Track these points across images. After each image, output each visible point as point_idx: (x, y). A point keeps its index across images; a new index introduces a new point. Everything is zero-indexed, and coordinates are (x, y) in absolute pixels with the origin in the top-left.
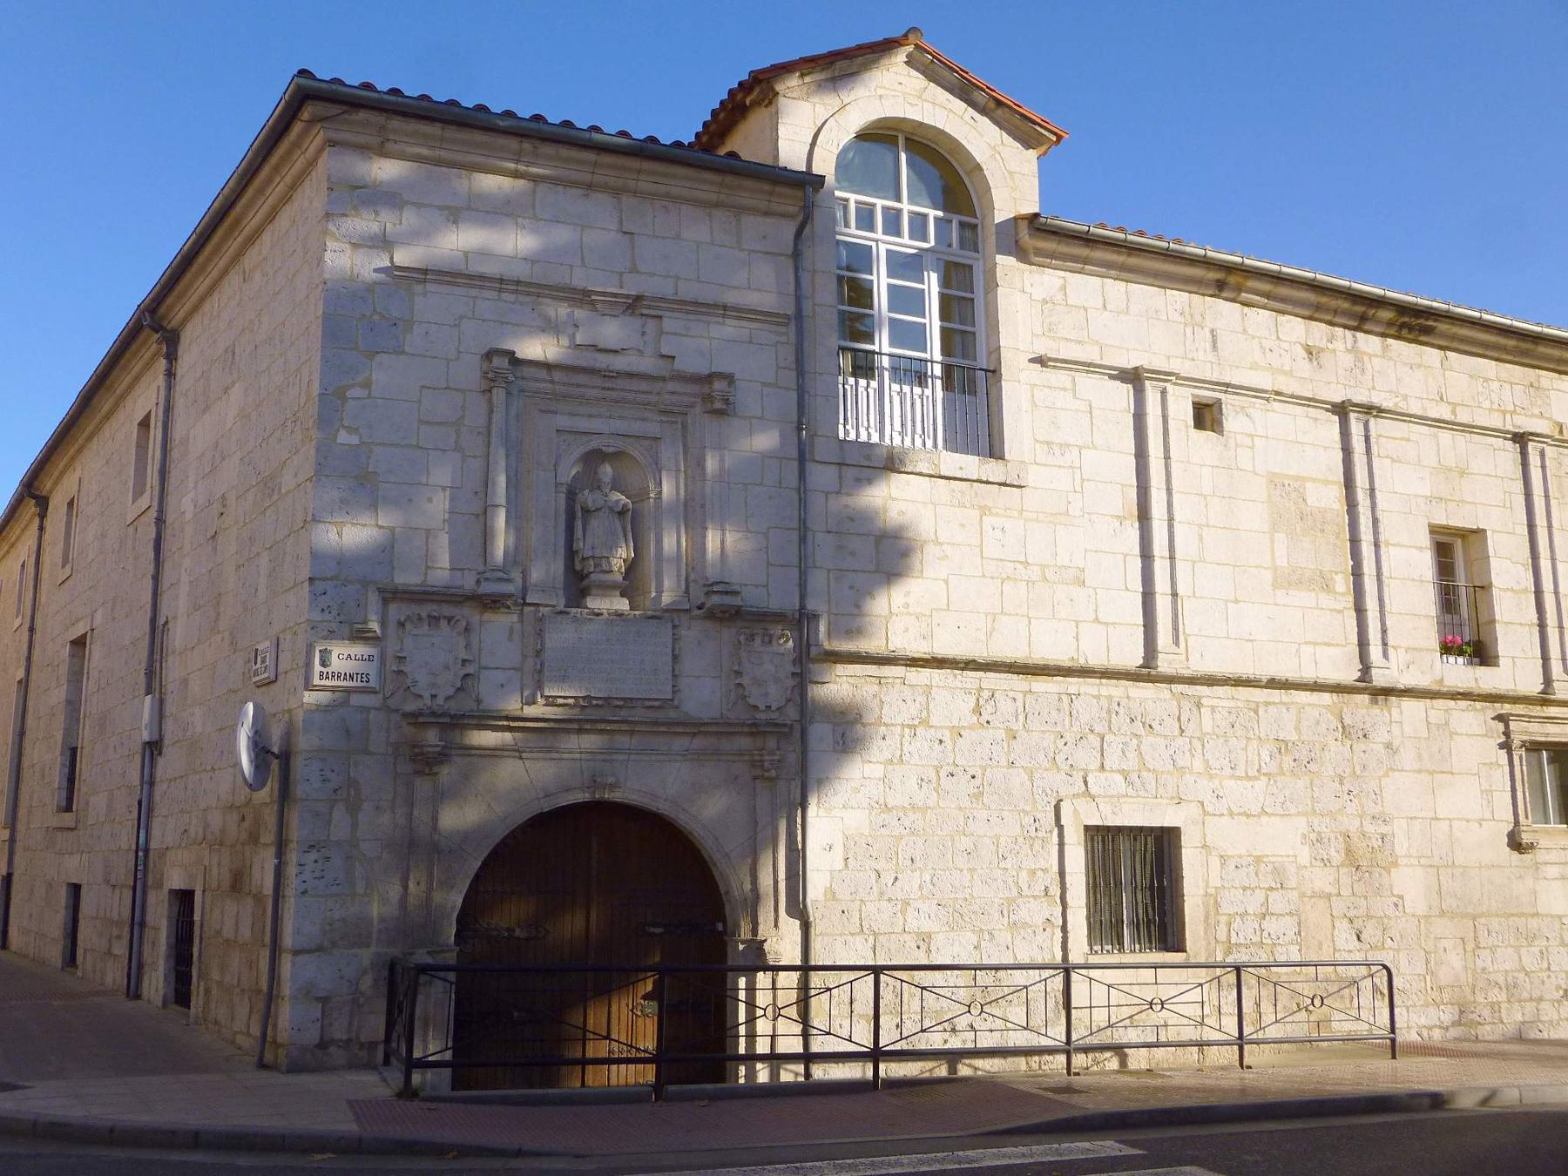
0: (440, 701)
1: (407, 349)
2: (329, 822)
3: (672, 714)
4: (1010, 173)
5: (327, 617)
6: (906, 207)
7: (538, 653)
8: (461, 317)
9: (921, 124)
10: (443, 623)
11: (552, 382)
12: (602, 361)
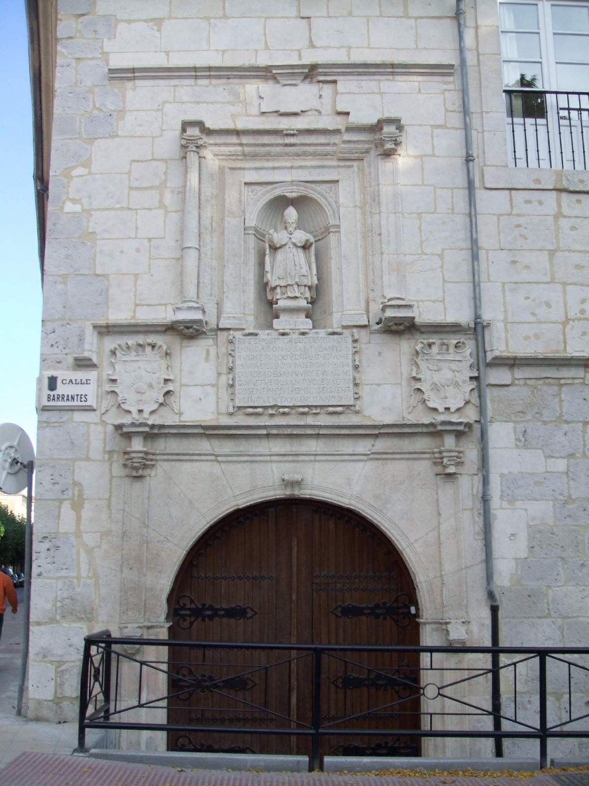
0: (146, 414)
1: (120, 133)
3: (355, 420)
5: (55, 350)
7: (231, 369)
8: (164, 102)
10: (148, 349)
11: (241, 145)
12: (284, 124)
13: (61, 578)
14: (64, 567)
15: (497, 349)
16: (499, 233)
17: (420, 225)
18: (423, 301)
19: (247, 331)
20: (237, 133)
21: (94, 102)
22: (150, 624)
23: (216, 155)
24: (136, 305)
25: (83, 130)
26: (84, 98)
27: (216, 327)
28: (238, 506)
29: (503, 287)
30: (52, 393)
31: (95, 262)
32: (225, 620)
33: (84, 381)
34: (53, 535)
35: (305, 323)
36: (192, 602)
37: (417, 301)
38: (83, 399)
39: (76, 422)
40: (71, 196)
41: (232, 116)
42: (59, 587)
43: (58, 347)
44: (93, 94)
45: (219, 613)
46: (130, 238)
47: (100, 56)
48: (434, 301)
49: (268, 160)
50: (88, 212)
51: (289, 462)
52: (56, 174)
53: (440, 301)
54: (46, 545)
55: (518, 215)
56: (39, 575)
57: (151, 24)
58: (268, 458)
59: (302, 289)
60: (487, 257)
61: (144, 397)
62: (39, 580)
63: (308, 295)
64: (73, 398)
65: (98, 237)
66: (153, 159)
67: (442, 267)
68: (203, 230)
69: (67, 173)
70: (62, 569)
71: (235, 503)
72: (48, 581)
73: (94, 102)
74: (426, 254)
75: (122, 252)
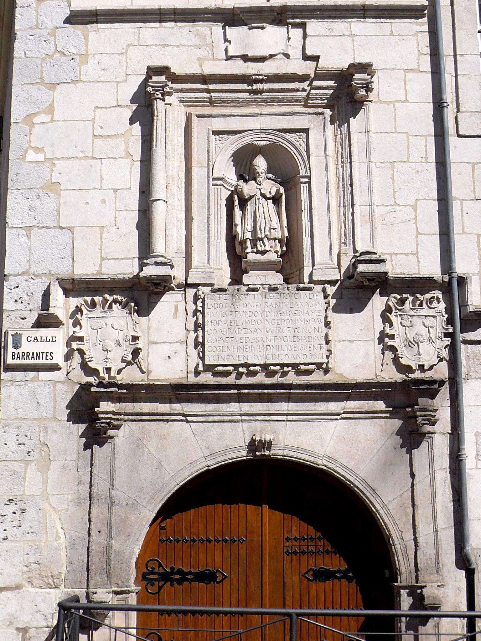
2: (24, 478)
3: (329, 378)
5: (19, 306)
8: (129, 45)
12: (252, 69)
15: (471, 305)
16: (474, 182)
17: (393, 174)
18: (396, 255)
19: (216, 287)
20: (204, 79)
22: (119, 590)
23: (181, 102)
24: (103, 259)
26: (45, 41)
27: (184, 282)
28: (208, 466)
30: (16, 351)
31: (58, 214)
35: (277, 279)
36: (160, 565)
37: (391, 255)
38: (49, 357)
40: (33, 145)
41: (199, 59)
43: (22, 302)
48: (407, 255)
49: (235, 106)
50: (51, 161)
51: (261, 421)
52: (18, 121)
58: (239, 418)
59: (272, 243)
60: (462, 207)
61: (110, 355)
62: (4, 544)
63: (278, 248)
67: (415, 218)
68: (170, 181)
69: (29, 119)
70: (28, 533)
71: (206, 464)
72: (14, 544)
74: (399, 205)
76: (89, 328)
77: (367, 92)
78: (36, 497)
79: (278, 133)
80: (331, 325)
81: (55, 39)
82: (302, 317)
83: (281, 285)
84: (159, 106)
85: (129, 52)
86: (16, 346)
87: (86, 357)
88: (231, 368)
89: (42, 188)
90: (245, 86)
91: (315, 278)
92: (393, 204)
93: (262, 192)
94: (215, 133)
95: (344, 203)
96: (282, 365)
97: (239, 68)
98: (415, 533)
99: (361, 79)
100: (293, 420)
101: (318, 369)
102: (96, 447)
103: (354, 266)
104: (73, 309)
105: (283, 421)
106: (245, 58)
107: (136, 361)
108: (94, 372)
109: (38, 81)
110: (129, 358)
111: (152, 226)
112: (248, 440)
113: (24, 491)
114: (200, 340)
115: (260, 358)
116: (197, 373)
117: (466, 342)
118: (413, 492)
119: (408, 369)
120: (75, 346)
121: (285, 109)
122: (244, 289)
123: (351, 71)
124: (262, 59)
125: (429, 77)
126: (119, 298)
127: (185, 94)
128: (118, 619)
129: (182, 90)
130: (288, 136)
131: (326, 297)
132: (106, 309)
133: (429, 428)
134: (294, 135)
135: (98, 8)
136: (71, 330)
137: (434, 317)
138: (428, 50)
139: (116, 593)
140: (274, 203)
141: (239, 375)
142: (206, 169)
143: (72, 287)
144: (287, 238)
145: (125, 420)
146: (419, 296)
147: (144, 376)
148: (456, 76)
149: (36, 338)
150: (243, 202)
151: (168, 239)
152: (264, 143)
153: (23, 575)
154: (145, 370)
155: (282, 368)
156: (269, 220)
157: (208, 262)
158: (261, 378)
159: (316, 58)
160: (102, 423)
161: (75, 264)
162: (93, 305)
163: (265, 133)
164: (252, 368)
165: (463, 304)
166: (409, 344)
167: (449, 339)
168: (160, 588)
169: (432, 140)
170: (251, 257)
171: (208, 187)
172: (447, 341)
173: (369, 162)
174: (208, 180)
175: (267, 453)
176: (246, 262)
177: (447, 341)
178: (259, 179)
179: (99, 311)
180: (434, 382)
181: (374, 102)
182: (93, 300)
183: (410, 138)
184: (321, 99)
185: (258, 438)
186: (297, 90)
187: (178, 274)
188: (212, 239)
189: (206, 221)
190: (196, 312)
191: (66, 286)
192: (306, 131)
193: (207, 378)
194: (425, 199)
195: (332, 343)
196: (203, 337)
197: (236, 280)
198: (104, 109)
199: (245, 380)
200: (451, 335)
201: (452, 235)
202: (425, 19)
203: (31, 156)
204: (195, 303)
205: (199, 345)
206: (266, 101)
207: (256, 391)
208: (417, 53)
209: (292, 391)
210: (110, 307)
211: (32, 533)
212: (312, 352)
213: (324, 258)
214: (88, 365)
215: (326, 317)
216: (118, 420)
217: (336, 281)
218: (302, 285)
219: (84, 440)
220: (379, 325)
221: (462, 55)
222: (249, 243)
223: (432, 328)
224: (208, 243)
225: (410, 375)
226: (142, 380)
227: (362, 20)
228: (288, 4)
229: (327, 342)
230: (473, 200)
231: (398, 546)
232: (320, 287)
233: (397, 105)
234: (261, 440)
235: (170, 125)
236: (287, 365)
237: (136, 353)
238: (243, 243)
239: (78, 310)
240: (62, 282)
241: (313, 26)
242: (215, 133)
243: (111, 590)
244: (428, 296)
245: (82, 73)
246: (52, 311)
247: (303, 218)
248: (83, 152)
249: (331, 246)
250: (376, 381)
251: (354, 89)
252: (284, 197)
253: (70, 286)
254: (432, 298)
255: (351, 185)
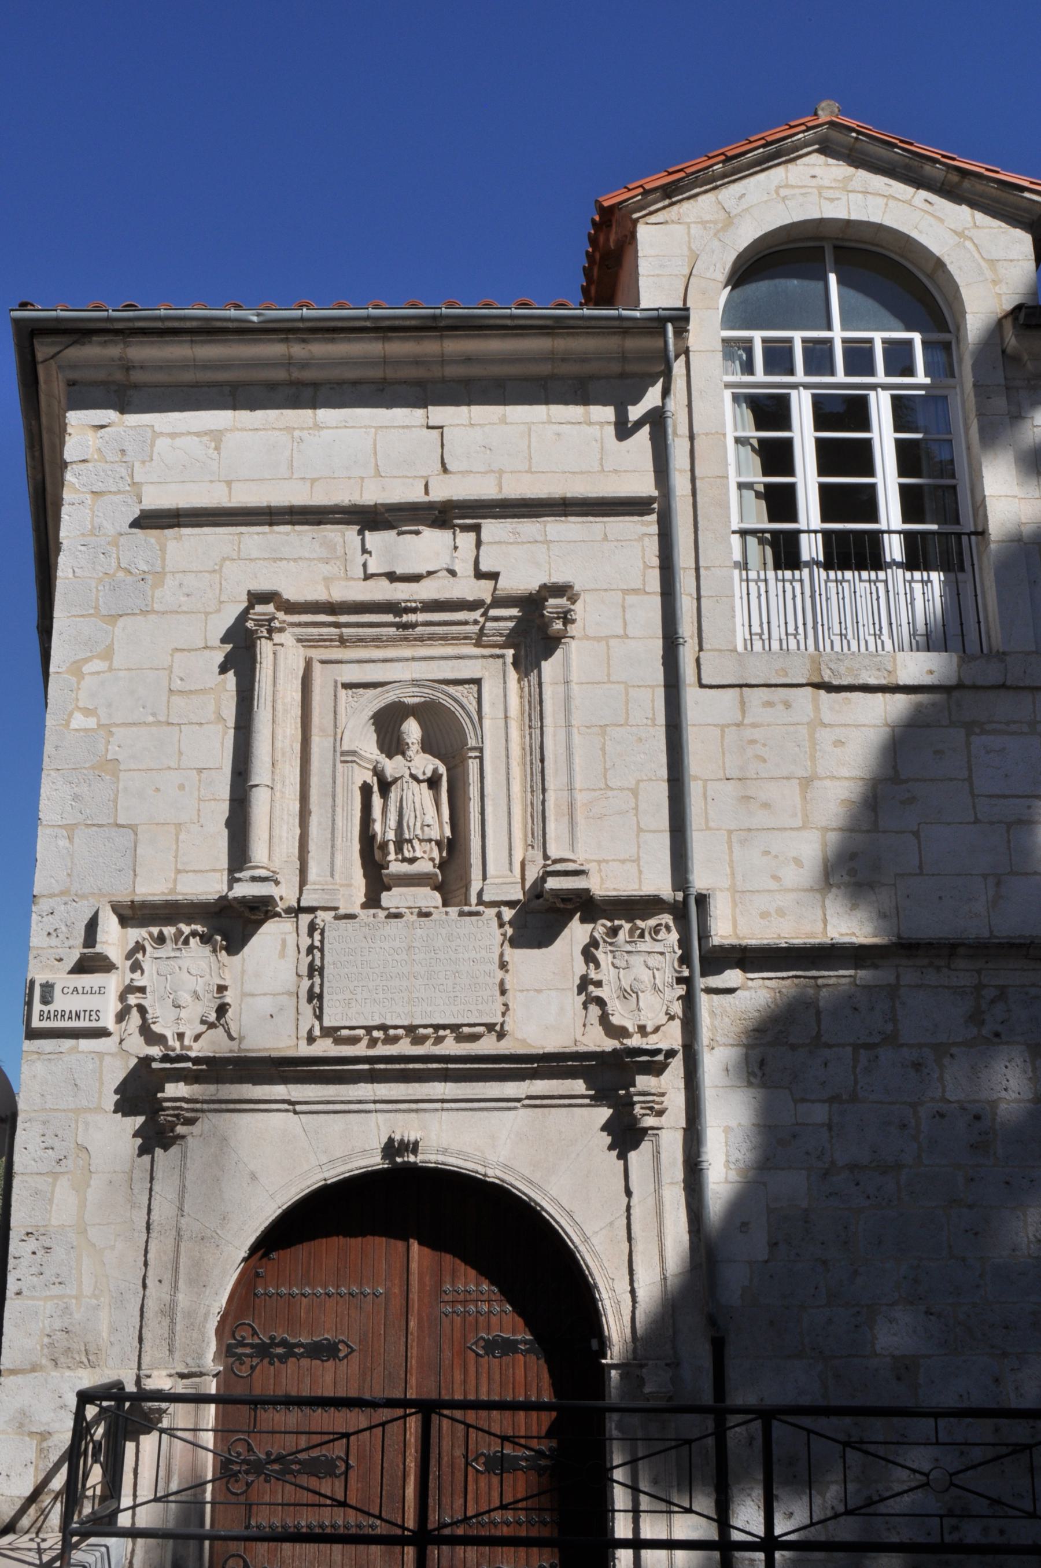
2: (51, 1200)
3: (504, 1047)
4: (992, 263)
5: (53, 941)
6: (838, 334)
8: (224, 559)
9: (848, 223)
12: (401, 592)
13: (52, 1297)
14: (57, 1281)
16: (723, 753)
17: (604, 744)
19: (342, 911)
20: (332, 608)
21: (118, 558)
23: (299, 641)
24: (178, 871)
25: (101, 602)
27: (296, 905)
29: (730, 838)
30: (46, 1008)
32: (305, 1362)
33: (96, 989)
34: (42, 1230)
37: (599, 862)
38: (94, 1017)
39: (83, 1052)
40: (81, 704)
42: (48, 1313)
44: (117, 546)
45: (296, 1350)
46: (169, 768)
47: (128, 488)
48: (623, 861)
49: (377, 647)
50: (107, 729)
52: (60, 670)
53: (633, 861)
54: (32, 1244)
55: (754, 725)
56: (19, 1294)
57: (205, 438)
58: (371, 1106)
59: (427, 846)
61: (183, 1014)
62: (17, 1301)
63: (436, 854)
64: (78, 1016)
65: (122, 767)
66: (206, 647)
67: (636, 808)
68: (279, 756)
69: (76, 669)
71: (321, 1176)
72: (30, 1302)
73: (118, 558)
74: (612, 789)
75: (157, 790)
76: (155, 974)
77: (565, 624)
78: (68, 1229)
79: (436, 685)
80: (509, 967)
81: (118, 551)
82: (466, 956)
83: (437, 908)
84: (265, 649)
85: (224, 570)
86: (46, 1000)
87: (149, 1016)
88: (362, 1032)
89: (93, 768)
90: (389, 618)
91: (486, 898)
92: (603, 786)
93: (413, 772)
94: (346, 686)
95: (532, 787)
96: (437, 1027)
97: (382, 591)
98: (632, 1282)
99: (557, 606)
100: (452, 1109)
101: (489, 1032)
102: (159, 1152)
103: (542, 879)
104: (131, 945)
105: (437, 1110)
106: (392, 577)
107: (222, 1021)
108: (159, 1039)
109: (92, 611)
110: (212, 1017)
111: (249, 824)
112: (384, 1140)
113: (49, 1220)
114: (317, 990)
115: (403, 1016)
116: (311, 1039)
117: (709, 991)
118: (628, 1218)
119: (621, 1032)
120: (132, 1000)
121: (449, 651)
122: (381, 914)
123: (544, 593)
124: (416, 578)
125: (657, 600)
126: (199, 928)
127: (304, 630)
128: (178, 1415)
129: (299, 625)
130: (451, 689)
131: (501, 925)
132: (180, 945)
133: (649, 1121)
134: (460, 688)
135: (180, 506)
136: (129, 975)
137: (662, 954)
138: (656, 562)
139: (182, 1376)
140: (430, 787)
141: (373, 1043)
142: (332, 739)
143: (132, 914)
144: (448, 838)
145: (202, 1111)
146: (639, 923)
147: (234, 1045)
148: (699, 599)
149: (76, 989)
150: (385, 786)
151: (272, 842)
152: (417, 700)
153: (42, 1348)
154: (234, 1034)
155: (436, 1032)
156: (425, 814)
157: (332, 875)
158: (405, 1047)
159: (494, 576)
160: (167, 1115)
161: (138, 879)
162: (161, 939)
163: (419, 686)
164: (392, 1032)
165: (704, 935)
166: (624, 994)
167: (684, 987)
168: (253, 1368)
169: (660, 692)
170: (396, 867)
171: (334, 766)
172: (681, 990)
173: (569, 726)
174: (334, 755)
175: (412, 1159)
176: (388, 875)
177: (681, 990)
178: (409, 753)
179: (170, 948)
180: (658, 1051)
181: (580, 639)
182: (161, 933)
183: (630, 690)
184: (501, 635)
185: (397, 1137)
186: (466, 623)
187: (286, 893)
188: (339, 842)
189: (330, 815)
190: (310, 950)
191: (122, 912)
192: (478, 682)
193: (325, 1048)
194: (651, 780)
195: (510, 994)
196: (322, 985)
197: (372, 901)
198: (186, 653)
199: (381, 1050)
200: (687, 981)
201: (688, 833)
202: (654, 517)
203: (79, 721)
204: (311, 934)
205: (315, 997)
206: (421, 639)
207: (397, 1066)
208: (641, 565)
209: (450, 1066)
210: (186, 942)
211: (60, 1283)
212: (480, 1007)
213: (502, 870)
214: (151, 1029)
215: (502, 955)
216: (193, 1110)
217: (518, 902)
218: (466, 909)
219: (139, 1141)
220: (580, 966)
221: (707, 568)
222: (392, 847)
223: (658, 969)
224: (333, 847)
225: (625, 1041)
226: (231, 1051)
227: (563, 519)
228: (454, 498)
229: (503, 992)
230: (721, 779)
231: (607, 1302)
232: (493, 911)
233: (613, 642)
234: (402, 1140)
235: (281, 675)
236: (444, 1027)
237: (222, 1010)
238: (384, 846)
239: (139, 947)
240: (116, 908)
241: (491, 528)
242: (346, 686)
243: (173, 1372)
244: (652, 922)
245: (155, 600)
246: (99, 948)
247: (472, 810)
248: (154, 715)
249: (510, 850)
250: (574, 1049)
251: (546, 620)
252: (445, 779)
253: (128, 912)
254: (660, 925)
255: (542, 761)
